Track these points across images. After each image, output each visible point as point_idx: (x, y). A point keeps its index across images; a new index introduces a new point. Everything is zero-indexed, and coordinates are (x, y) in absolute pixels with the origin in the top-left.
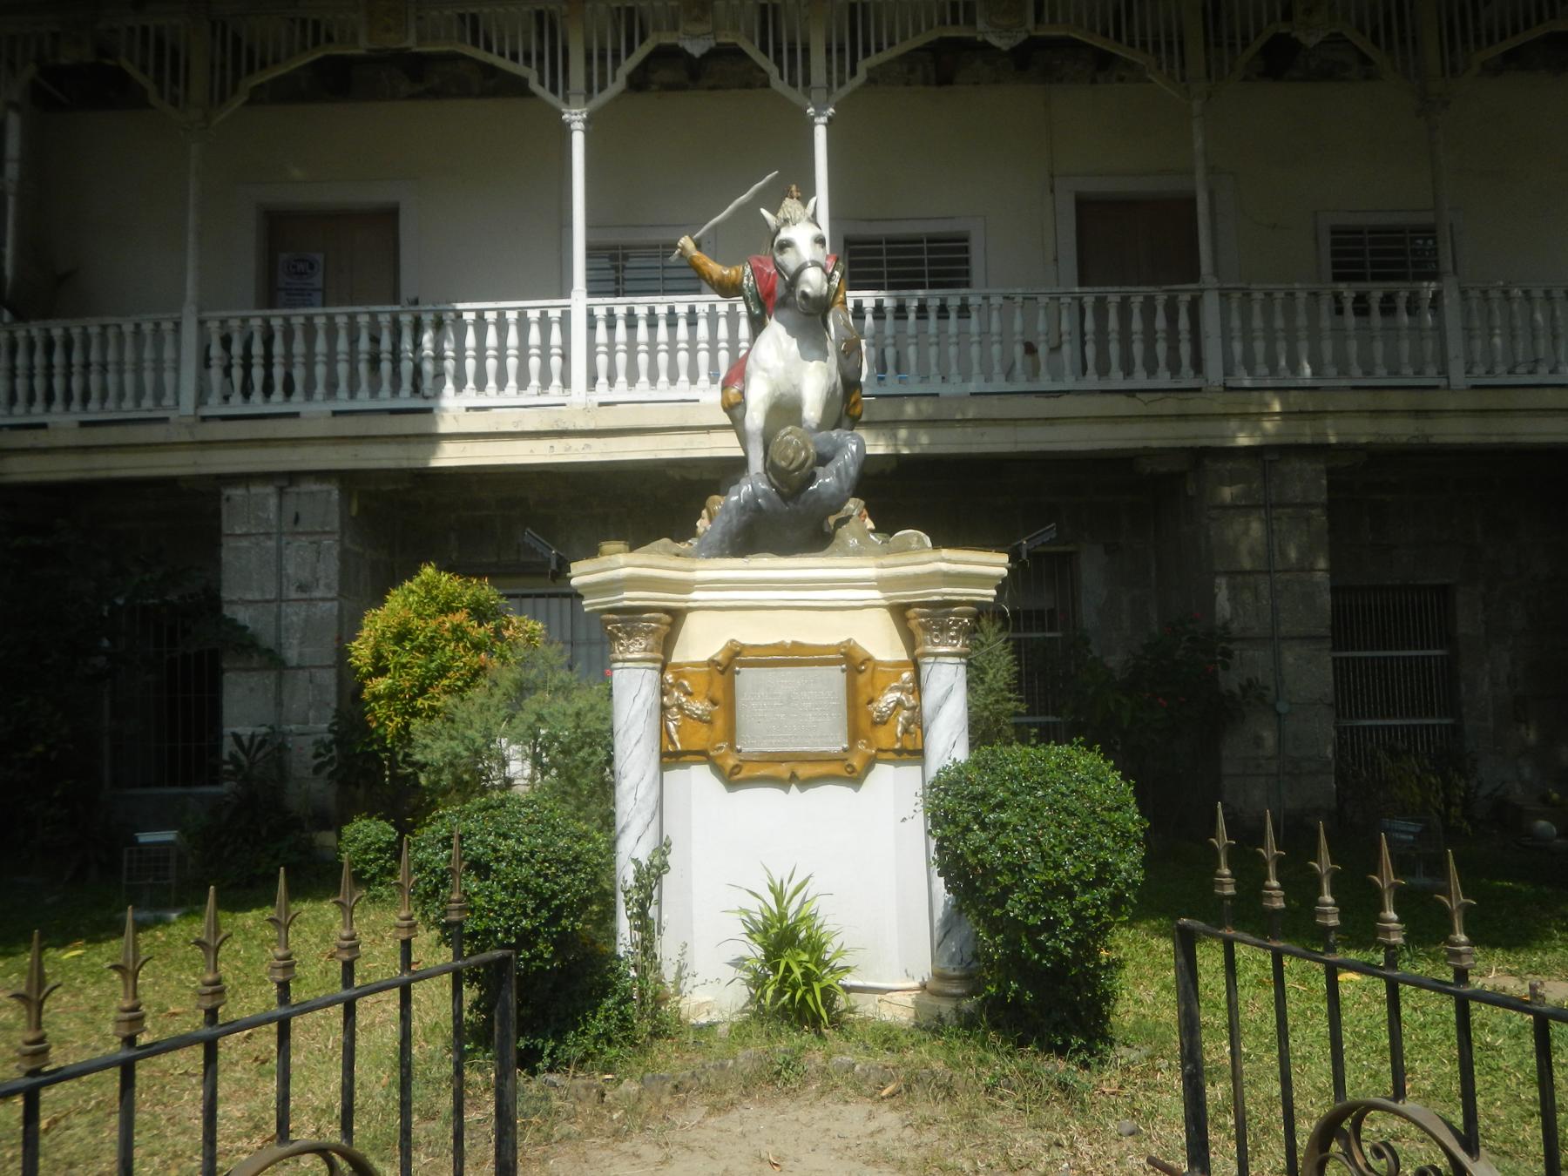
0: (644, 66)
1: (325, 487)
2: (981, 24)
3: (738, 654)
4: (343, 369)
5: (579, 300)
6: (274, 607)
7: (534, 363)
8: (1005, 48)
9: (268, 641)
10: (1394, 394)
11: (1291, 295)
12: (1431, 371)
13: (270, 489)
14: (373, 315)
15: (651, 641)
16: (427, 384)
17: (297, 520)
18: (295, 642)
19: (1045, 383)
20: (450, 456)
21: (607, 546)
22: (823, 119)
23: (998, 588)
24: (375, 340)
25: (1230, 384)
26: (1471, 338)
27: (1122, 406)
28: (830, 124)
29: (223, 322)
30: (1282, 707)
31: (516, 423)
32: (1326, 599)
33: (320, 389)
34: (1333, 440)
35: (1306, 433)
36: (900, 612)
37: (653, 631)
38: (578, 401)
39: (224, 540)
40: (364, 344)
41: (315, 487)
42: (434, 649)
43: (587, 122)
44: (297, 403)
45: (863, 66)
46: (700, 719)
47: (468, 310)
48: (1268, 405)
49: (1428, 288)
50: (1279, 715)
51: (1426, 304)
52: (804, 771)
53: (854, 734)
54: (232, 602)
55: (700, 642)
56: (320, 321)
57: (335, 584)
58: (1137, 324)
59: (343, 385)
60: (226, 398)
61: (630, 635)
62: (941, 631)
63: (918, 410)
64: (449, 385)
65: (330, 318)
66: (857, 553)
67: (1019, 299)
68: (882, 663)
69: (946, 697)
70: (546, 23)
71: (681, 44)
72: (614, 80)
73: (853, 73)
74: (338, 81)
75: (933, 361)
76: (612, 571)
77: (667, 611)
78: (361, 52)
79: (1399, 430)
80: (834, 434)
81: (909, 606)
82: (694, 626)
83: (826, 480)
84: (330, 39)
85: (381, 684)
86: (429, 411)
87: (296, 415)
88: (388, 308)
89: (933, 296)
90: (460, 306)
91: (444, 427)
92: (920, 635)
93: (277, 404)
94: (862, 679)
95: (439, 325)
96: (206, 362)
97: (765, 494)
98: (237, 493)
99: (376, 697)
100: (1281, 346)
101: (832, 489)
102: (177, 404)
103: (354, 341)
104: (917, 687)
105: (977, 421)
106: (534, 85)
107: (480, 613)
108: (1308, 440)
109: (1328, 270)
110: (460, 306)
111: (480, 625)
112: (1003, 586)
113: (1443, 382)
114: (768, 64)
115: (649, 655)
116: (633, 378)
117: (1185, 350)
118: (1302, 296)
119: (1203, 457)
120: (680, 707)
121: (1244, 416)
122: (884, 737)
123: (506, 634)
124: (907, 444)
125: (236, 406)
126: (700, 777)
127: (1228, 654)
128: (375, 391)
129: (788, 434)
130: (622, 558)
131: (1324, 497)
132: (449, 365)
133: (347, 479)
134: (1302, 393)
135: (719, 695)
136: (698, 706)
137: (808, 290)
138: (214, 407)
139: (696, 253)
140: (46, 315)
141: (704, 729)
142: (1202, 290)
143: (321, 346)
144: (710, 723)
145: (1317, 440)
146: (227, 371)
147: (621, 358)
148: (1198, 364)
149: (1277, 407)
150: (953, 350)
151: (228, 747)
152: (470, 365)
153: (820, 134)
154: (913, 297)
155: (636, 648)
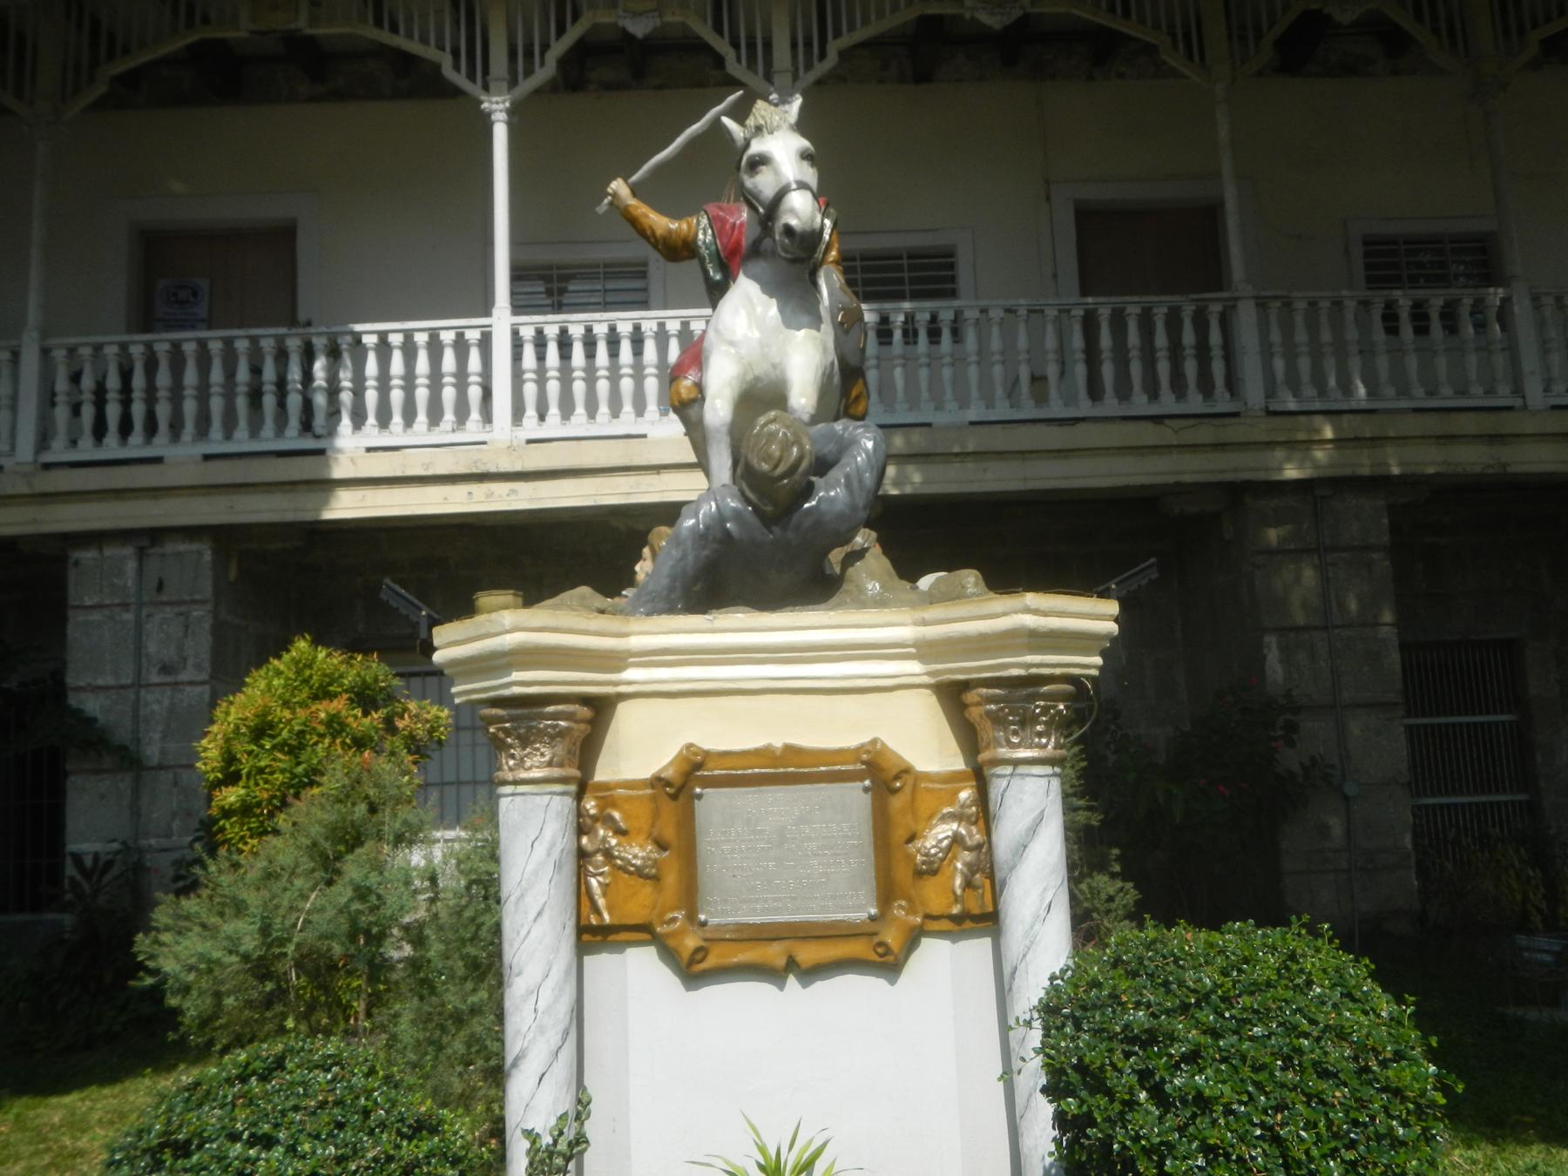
1: (195, 546)
3: (699, 766)
4: (216, 405)
5: (502, 319)
6: (131, 694)
7: (449, 394)
8: (997, 26)
9: (122, 735)
10: (1463, 417)
11: (1338, 304)
12: (1504, 389)
13: (129, 551)
14: (254, 340)
15: (560, 749)
16: (319, 421)
17: (160, 586)
18: (157, 736)
19: (1056, 409)
20: (346, 507)
21: (485, 599)
23: (1103, 654)
24: (256, 371)
25: (1274, 407)
27: (1149, 434)
29: (72, 351)
30: (1350, 789)
31: (427, 466)
32: (1394, 658)
34: (1396, 470)
35: (1363, 463)
36: (953, 695)
37: (562, 734)
38: (501, 438)
39: (71, 613)
40: (243, 374)
41: (182, 547)
42: (301, 747)
43: (511, 112)
44: (160, 446)
45: (833, 47)
46: (639, 873)
47: (369, 333)
48: (1318, 431)
49: (1496, 295)
50: (1346, 798)
51: (1492, 314)
52: (808, 954)
53: (887, 893)
54: (79, 689)
55: (638, 750)
56: (189, 348)
57: (207, 665)
58: (1161, 340)
60: (74, 443)
61: (525, 742)
62: (1023, 723)
64: (346, 422)
66: (880, 603)
67: (1023, 312)
68: (927, 776)
69: (1033, 830)
71: (621, 23)
72: (542, 64)
73: (823, 55)
74: (221, 77)
75: (924, 385)
76: (499, 637)
78: (243, 34)
79: (1472, 459)
80: (838, 426)
81: (966, 686)
82: (628, 722)
83: (831, 494)
84: (206, 21)
85: (231, 796)
86: (321, 452)
87: (158, 460)
88: (272, 331)
89: (922, 310)
90: (358, 328)
91: (338, 472)
92: (987, 731)
93: (136, 446)
94: (897, 802)
95: (334, 354)
96: (49, 399)
97: (737, 516)
98: (87, 555)
99: (227, 813)
100: (1330, 365)
101: (839, 506)
102: (13, 447)
103: (230, 374)
104: (984, 813)
105: (978, 455)
106: (448, 71)
107: (365, 698)
108: (1366, 471)
110: (358, 328)
111: (366, 714)
112: (1112, 650)
113: (1518, 402)
114: (722, 46)
115: (556, 772)
116: (567, 409)
117: (1218, 368)
118: (1350, 305)
119: (1241, 495)
120: (608, 854)
121: (1291, 445)
122: (937, 896)
123: (400, 724)
124: (896, 484)
125: (87, 450)
126: (638, 972)
127: (1291, 727)
128: (255, 429)
129: (767, 422)
130: (508, 617)
131: (1386, 539)
132: (346, 397)
133: (224, 537)
134: (1359, 417)
135: (669, 833)
136: (637, 852)
137: (794, 222)
138: (59, 451)
139: (632, 202)
141: (647, 890)
142: (1236, 299)
143: (190, 377)
144: (656, 879)
145: (1378, 471)
146: (76, 410)
148: (1232, 384)
149: (1328, 433)
150: (947, 372)
151: (70, 870)
152: (371, 397)
154: (898, 310)
155: (536, 763)
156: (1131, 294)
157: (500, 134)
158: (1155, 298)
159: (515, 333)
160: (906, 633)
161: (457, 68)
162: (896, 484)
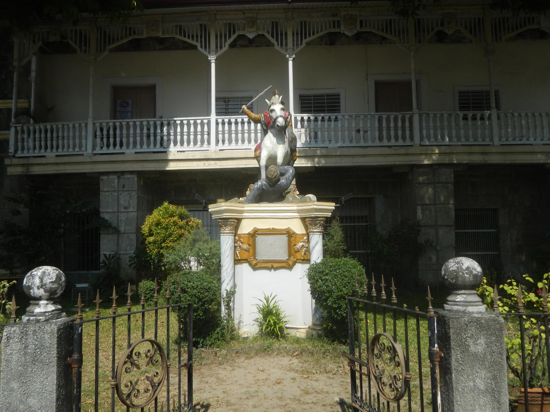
0: (235, 40)
1: (133, 176)
2: (342, 28)
3: (257, 231)
4: (138, 139)
5: (213, 117)
6: (116, 214)
7: (199, 137)
9: (114, 225)
11: (442, 115)
12: (488, 140)
13: (115, 177)
14: (148, 122)
15: (232, 228)
16: (165, 144)
17: (124, 187)
18: (123, 225)
19: (362, 144)
20: (172, 167)
21: (219, 200)
22: (291, 59)
24: (149, 129)
26: (501, 129)
27: (387, 151)
28: (293, 60)
29: (101, 124)
30: (438, 248)
32: (453, 213)
33: (131, 145)
34: (455, 162)
35: (447, 160)
36: (303, 219)
37: (232, 225)
38: (213, 150)
39: (101, 193)
40: (145, 131)
41: (129, 176)
42: (168, 228)
43: (216, 60)
44: (124, 149)
45: (304, 41)
46: (245, 250)
47: (178, 120)
48: (434, 151)
49: (487, 113)
50: (437, 250)
51: (486, 118)
52: (275, 265)
53: (290, 255)
54: (103, 212)
55: (246, 228)
56: (131, 124)
57: (136, 207)
58: (392, 125)
59: (138, 144)
60: (102, 148)
61: (225, 226)
62: (315, 225)
63: (321, 152)
64: (172, 144)
65: (135, 122)
66: (292, 202)
67: (354, 117)
68: (298, 234)
69: (316, 244)
70: (204, 28)
71: (246, 35)
72: (225, 46)
73: (301, 44)
74: (137, 45)
75: (326, 137)
76: (221, 207)
77: (236, 219)
78: (144, 37)
79: (477, 159)
80: (286, 167)
81: (306, 218)
82: (244, 223)
83: (283, 181)
84: (134, 33)
85: (151, 239)
86: (165, 152)
87: (123, 153)
88: (153, 119)
90: (175, 119)
91: (170, 158)
92: (309, 226)
93: (118, 150)
94: (292, 239)
95: (169, 124)
96: (95, 136)
97: (265, 185)
98: (105, 178)
99: (150, 243)
100: (439, 132)
101: (284, 184)
102: (86, 150)
103: (142, 130)
104: (308, 241)
105: (340, 156)
107: (181, 217)
108: (447, 162)
109: (457, 105)
110: (175, 119)
111: (182, 221)
112: (334, 212)
113: (491, 143)
114: (274, 41)
115: (231, 232)
116: (230, 142)
117: (407, 133)
118: (446, 116)
119: (413, 167)
120: (240, 247)
121: (426, 154)
122: (299, 256)
123: (190, 224)
124: (317, 163)
125: (105, 150)
126: (245, 268)
127: (419, 231)
128: (148, 145)
129: (272, 168)
130: (223, 204)
131: (453, 180)
132: (172, 137)
133: (140, 174)
134: (446, 147)
135: (251, 243)
136: (245, 246)
137: (279, 124)
138: (98, 151)
139: (247, 110)
140: (45, 122)
141: (247, 253)
142: (413, 114)
143: (131, 131)
144: (248, 251)
145: (450, 162)
146: (102, 139)
147: (227, 136)
148: (412, 138)
149: (437, 151)
150: (333, 133)
151: (102, 258)
152: (179, 137)
153: (291, 63)
155: (227, 230)
156: (384, 112)
157: (213, 66)
158: (391, 113)
159: (217, 121)
160: (295, 208)
161: (201, 47)
162: (317, 163)
